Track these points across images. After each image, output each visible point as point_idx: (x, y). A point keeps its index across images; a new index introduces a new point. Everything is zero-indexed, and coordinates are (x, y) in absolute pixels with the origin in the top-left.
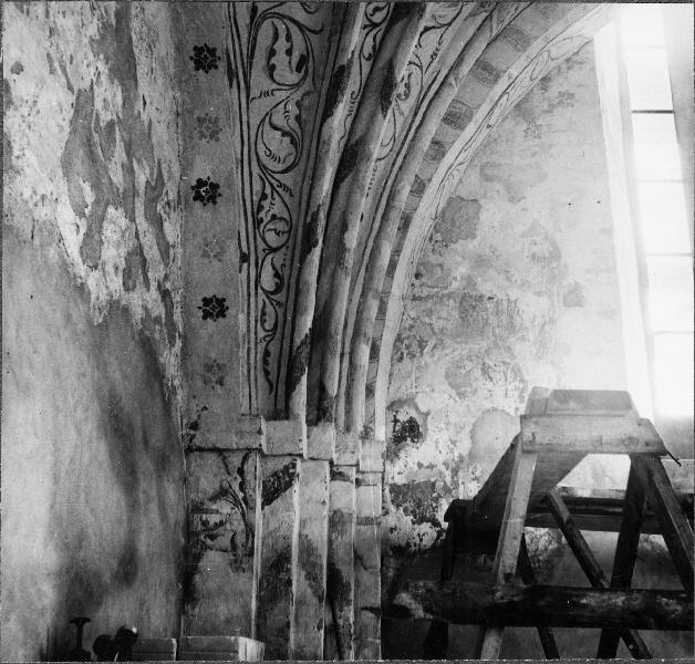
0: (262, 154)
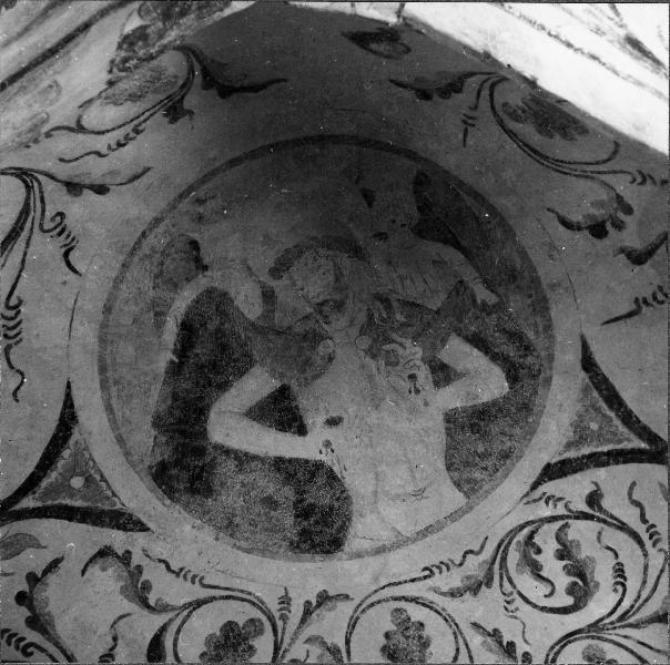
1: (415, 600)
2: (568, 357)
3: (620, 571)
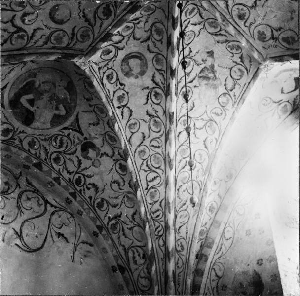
0: (142, 288)
1: (36, 138)
2: (75, 114)
3: (67, 146)
